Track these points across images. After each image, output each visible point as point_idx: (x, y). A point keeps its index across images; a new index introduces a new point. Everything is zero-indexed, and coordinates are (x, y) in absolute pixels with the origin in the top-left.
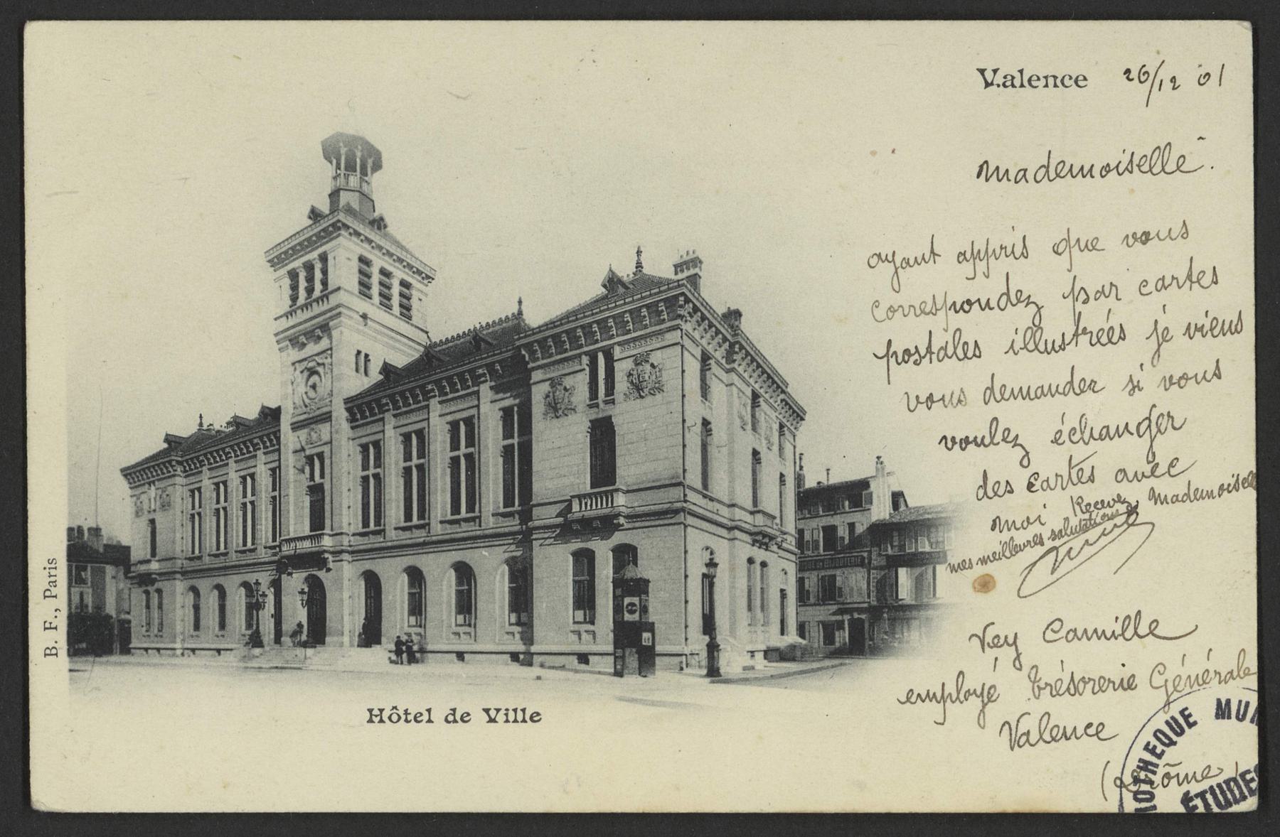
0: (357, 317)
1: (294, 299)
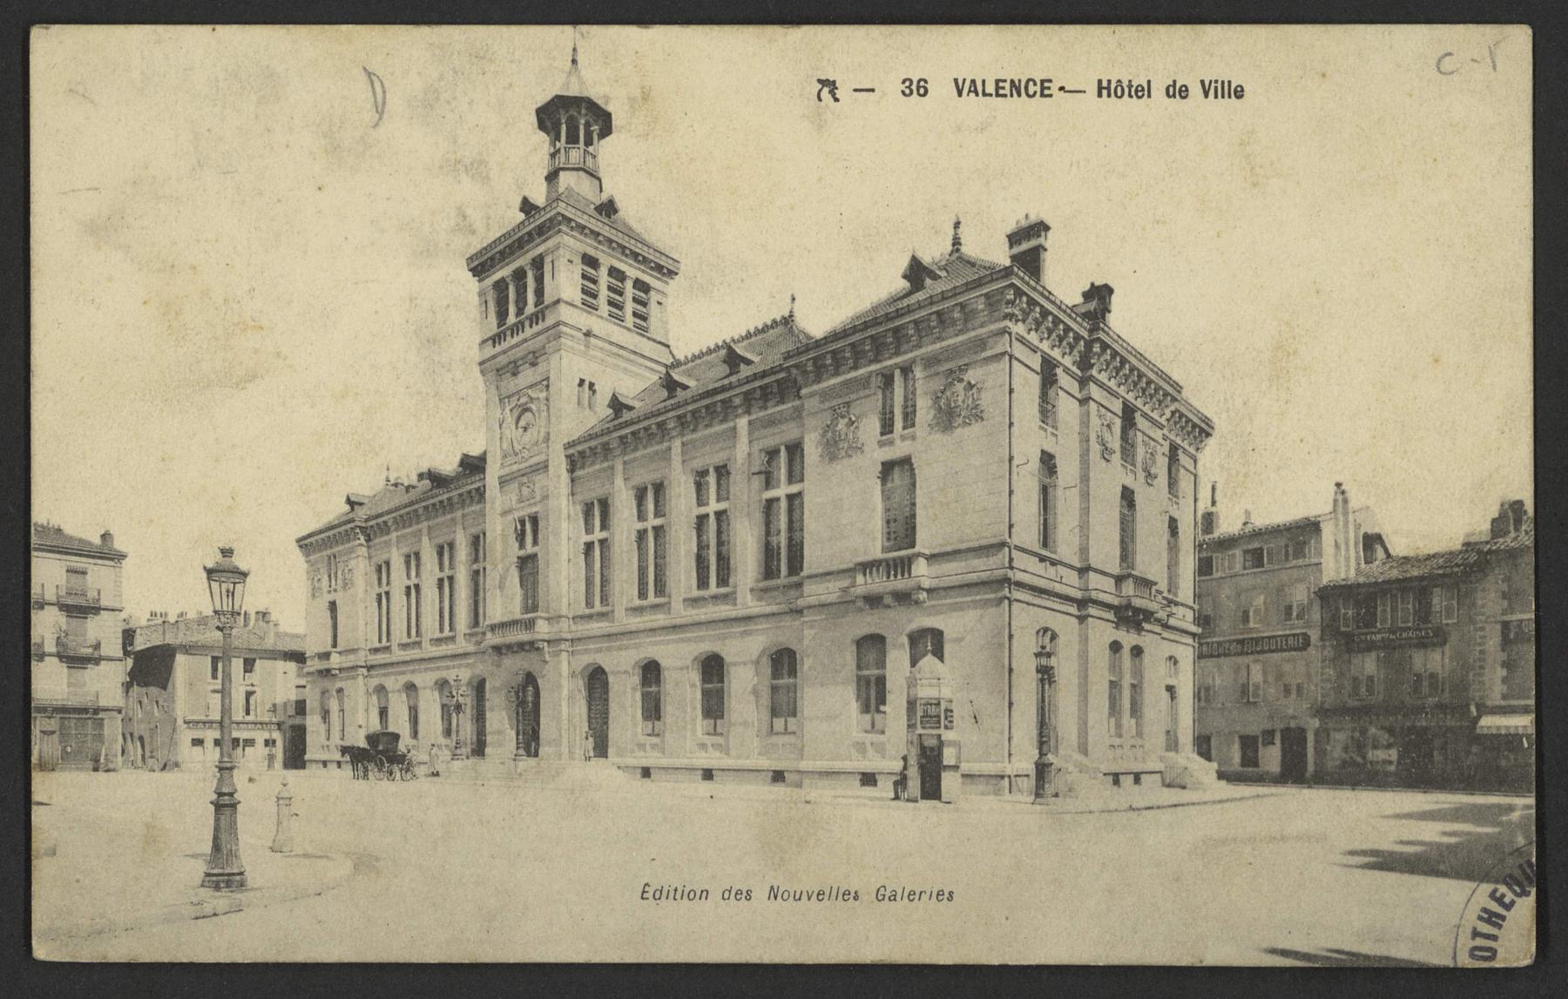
0: (580, 335)
1: (502, 315)
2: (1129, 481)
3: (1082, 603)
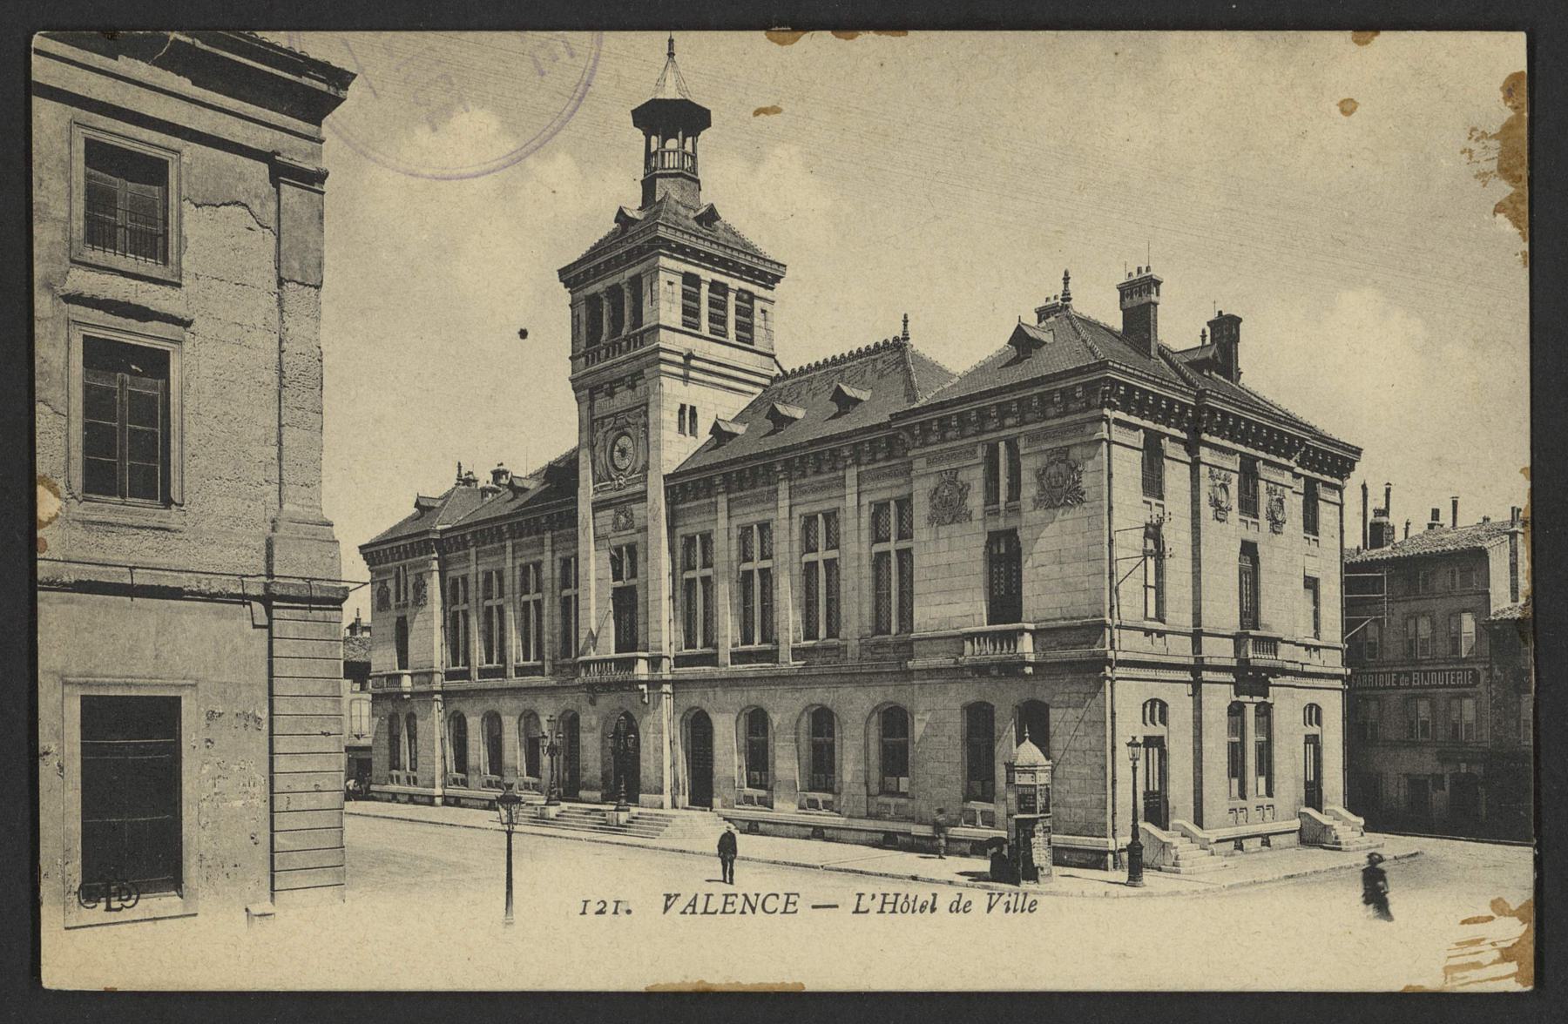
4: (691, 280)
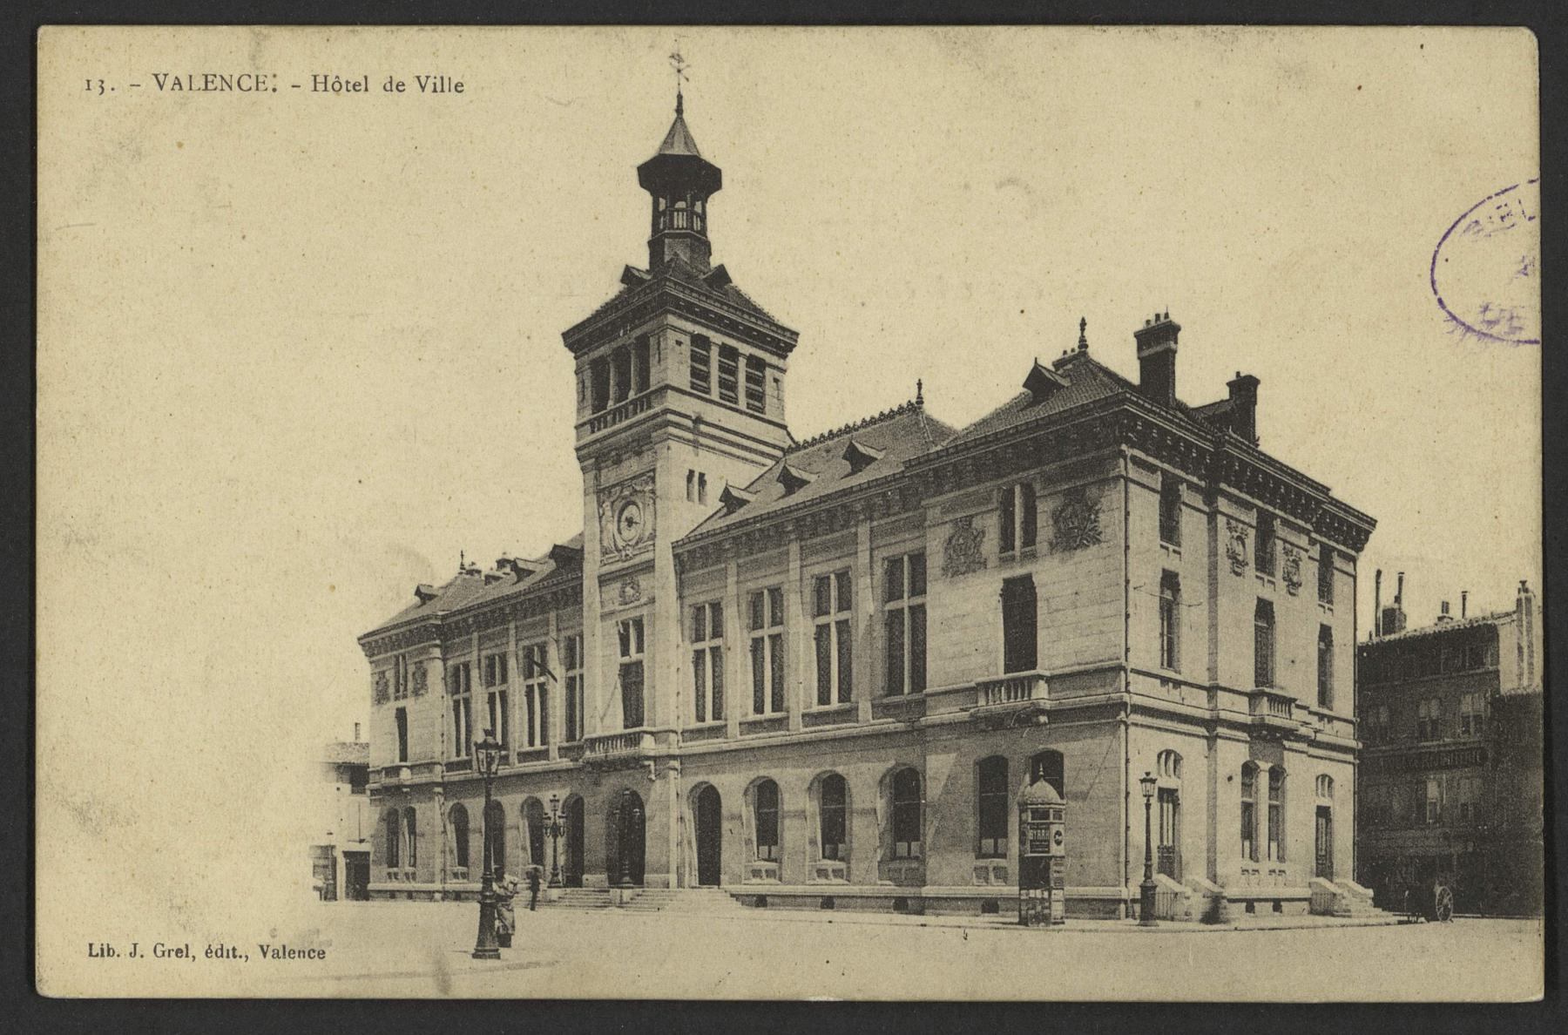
0: (689, 423)
1: (600, 401)
2: (1267, 594)
3: (1211, 724)
4: (700, 342)
